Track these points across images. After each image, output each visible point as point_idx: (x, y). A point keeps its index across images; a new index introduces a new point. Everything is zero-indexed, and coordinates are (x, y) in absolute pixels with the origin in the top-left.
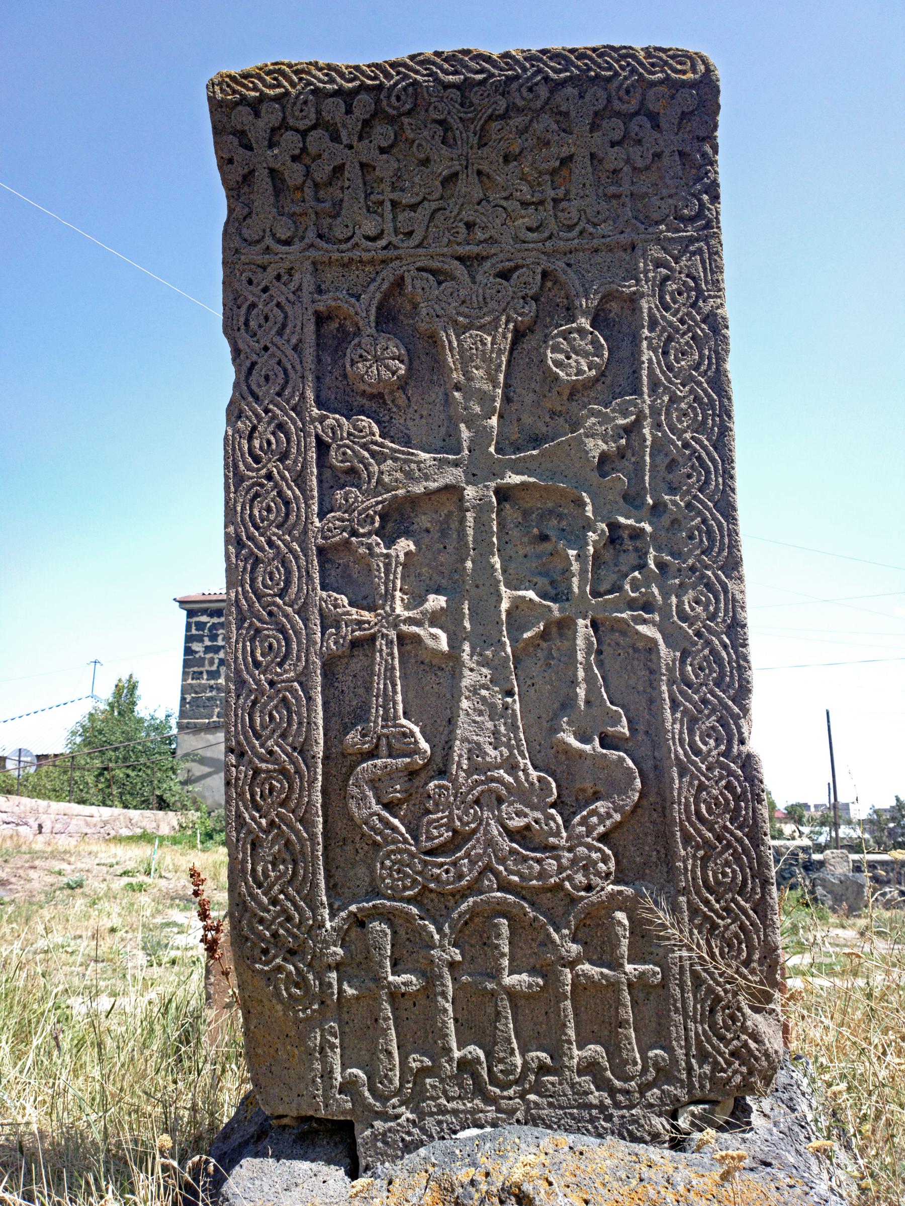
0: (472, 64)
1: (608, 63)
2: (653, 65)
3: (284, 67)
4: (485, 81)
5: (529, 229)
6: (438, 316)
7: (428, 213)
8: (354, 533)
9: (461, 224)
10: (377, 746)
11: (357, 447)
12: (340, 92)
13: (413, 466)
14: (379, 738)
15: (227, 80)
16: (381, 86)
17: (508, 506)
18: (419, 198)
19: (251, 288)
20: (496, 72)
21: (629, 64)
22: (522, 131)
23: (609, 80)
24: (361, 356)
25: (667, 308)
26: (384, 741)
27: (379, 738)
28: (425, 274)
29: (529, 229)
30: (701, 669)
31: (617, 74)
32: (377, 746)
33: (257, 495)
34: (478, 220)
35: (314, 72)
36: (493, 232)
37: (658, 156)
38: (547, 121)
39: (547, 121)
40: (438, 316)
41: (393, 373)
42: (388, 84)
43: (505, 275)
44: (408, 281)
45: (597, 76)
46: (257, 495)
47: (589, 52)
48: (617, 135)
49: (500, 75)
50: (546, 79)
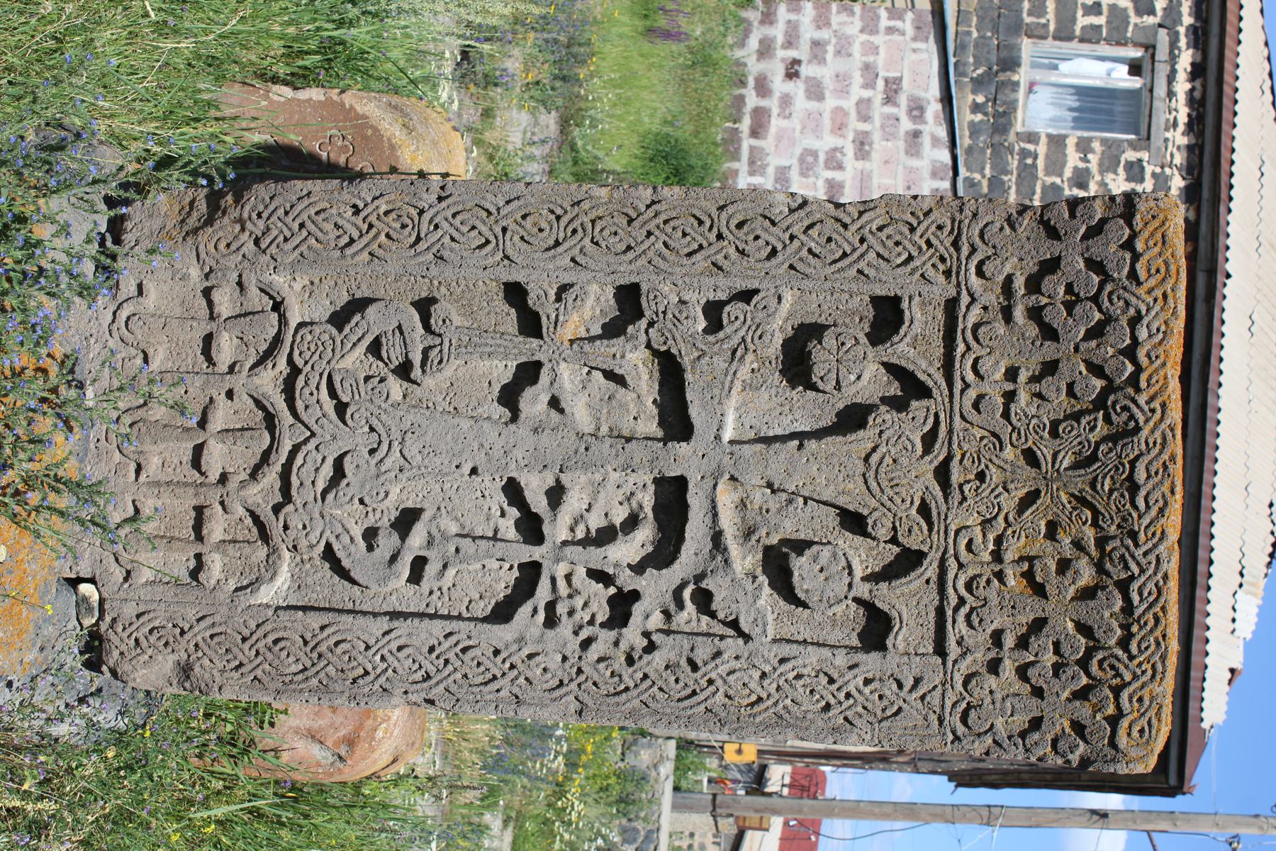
0: (1157, 495)
1: (1147, 648)
2: (1140, 700)
3: (1173, 281)
4: (1136, 508)
5: (971, 541)
6: (881, 432)
7: (997, 430)
8: (651, 324)
9: (983, 466)
10: (433, 333)
11: (742, 333)
12: (1135, 342)
13: (716, 391)
14: (440, 335)
15: (1161, 216)
16: (1138, 390)
17: (672, 489)
18: (1014, 421)
19: (933, 228)
20: (1146, 521)
21: (1143, 672)
22: (1078, 545)
23: (1126, 649)
24: (843, 344)
25: (867, 682)
26: (438, 341)
27: (440, 335)
28: (931, 420)
29: (971, 541)
30: (479, 664)
31: (1131, 658)
32: (433, 333)
33: (701, 223)
34: (984, 486)
35: (1163, 317)
36: (970, 501)
37: (1038, 692)
38: (1086, 575)
39: (1086, 575)
40: (881, 432)
41: (822, 378)
42: (1142, 399)
43: (924, 510)
44: (925, 402)
45: (1131, 635)
46: (701, 223)
47: (1160, 628)
48: (1066, 650)
49: (1140, 525)
50: (1132, 578)
